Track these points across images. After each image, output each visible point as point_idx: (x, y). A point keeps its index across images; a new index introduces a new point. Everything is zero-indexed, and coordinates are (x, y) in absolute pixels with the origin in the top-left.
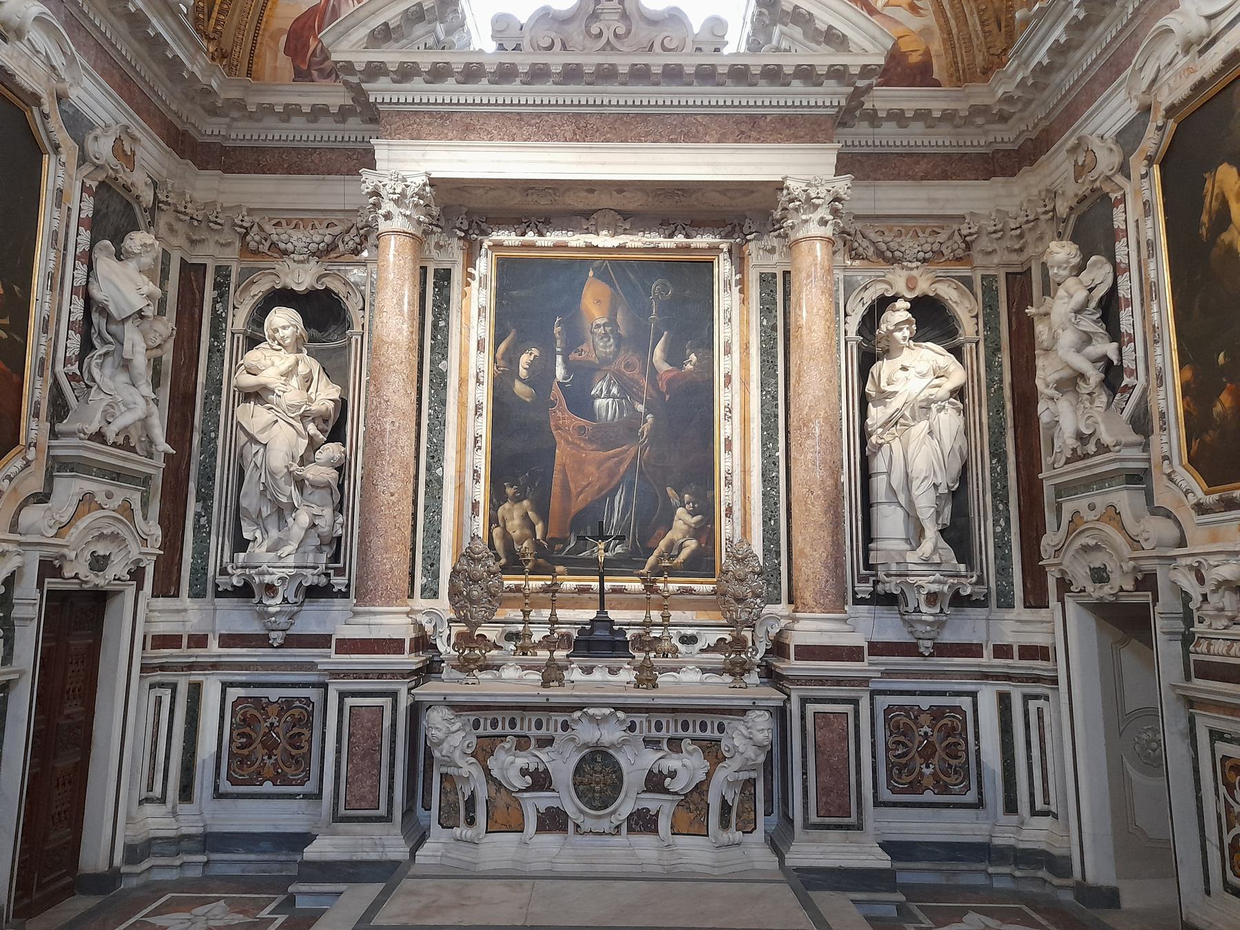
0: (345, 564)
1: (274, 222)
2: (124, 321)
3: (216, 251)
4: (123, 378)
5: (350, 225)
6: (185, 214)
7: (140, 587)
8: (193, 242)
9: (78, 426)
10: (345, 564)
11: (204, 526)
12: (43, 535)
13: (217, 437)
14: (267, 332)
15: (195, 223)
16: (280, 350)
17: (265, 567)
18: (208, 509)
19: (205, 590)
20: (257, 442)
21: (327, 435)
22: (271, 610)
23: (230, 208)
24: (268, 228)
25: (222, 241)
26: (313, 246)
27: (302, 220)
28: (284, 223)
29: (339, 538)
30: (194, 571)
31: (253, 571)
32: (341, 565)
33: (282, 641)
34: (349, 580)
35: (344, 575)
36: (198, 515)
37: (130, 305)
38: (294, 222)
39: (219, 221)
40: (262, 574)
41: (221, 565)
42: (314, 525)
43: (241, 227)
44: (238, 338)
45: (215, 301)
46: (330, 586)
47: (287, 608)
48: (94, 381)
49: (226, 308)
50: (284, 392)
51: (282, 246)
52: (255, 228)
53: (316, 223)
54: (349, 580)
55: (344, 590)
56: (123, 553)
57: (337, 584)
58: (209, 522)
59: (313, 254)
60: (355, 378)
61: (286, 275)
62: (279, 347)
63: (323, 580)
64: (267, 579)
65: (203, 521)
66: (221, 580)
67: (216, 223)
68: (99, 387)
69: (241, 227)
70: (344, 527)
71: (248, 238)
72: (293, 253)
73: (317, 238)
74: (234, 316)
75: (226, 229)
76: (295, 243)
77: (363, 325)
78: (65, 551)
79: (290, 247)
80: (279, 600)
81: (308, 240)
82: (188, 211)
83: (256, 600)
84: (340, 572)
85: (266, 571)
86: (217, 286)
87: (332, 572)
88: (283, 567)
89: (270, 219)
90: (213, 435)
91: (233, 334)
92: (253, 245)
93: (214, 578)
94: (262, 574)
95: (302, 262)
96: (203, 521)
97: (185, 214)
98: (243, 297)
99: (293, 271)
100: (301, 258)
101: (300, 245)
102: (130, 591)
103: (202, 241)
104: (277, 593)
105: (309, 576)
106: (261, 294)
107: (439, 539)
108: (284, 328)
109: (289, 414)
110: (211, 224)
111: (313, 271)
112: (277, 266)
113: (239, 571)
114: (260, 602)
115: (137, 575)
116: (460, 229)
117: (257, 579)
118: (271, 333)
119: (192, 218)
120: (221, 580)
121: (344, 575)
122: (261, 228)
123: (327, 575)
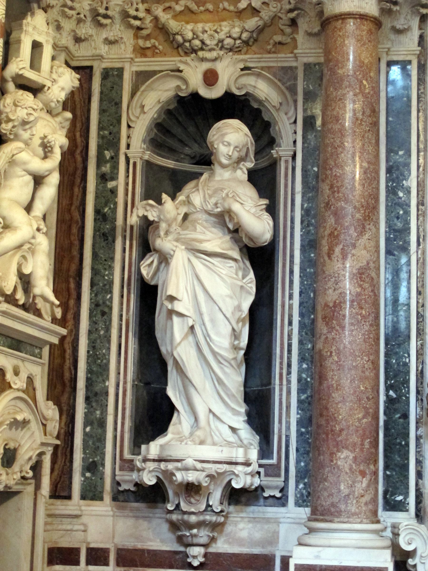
3: (104, 49)
7: (38, 487)
8: (78, 40)
17: (190, 462)
25: (111, 38)
26: (228, 41)
32: (274, 461)
33: (202, 560)
35: (279, 476)
39: (109, 13)
40: (186, 469)
55: (278, 495)
72: (202, 49)
79: (197, 43)
93: (114, 475)
94: (186, 469)
100: (214, 54)
102: (30, 489)
105: (242, 476)
121: (279, 476)
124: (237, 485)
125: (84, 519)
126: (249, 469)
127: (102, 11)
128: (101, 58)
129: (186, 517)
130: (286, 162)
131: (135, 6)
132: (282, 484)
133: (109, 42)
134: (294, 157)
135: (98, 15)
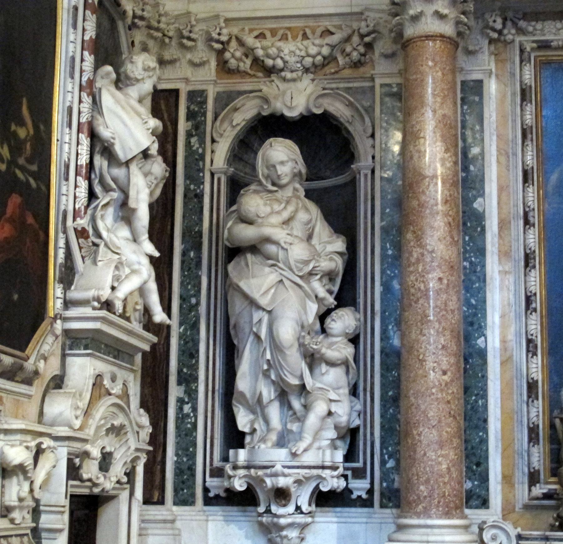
0: (365, 463)
1: (256, 33)
2: (127, 164)
3: (188, 72)
4: (124, 232)
5: (350, 32)
6: (158, 29)
7: (132, 494)
9: (90, 294)
10: (365, 463)
11: (188, 415)
12: (71, 427)
13: (198, 304)
14: (261, 170)
15: (167, 40)
16: (276, 191)
17: (278, 468)
18: (192, 394)
19: (193, 495)
20: (259, 307)
21: (334, 296)
22: (283, 521)
23: (204, 20)
24: (250, 40)
25: (197, 60)
26: (308, 61)
27: (289, 29)
28: (268, 34)
29: (357, 429)
30: (179, 471)
31: (260, 473)
32: (360, 465)
34: (372, 483)
36: (181, 402)
37: (138, 143)
38: (281, 32)
39: (193, 36)
40: (276, 475)
41: (211, 464)
42: (330, 414)
43: (218, 41)
44: (219, 180)
45: (189, 135)
46: (348, 491)
47: (300, 519)
48: (100, 236)
49: (202, 142)
50: (291, 244)
51: (269, 62)
52: (234, 44)
53: (308, 31)
54: (372, 483)
55: (364, 496)
56: (123, 449)
57: (358, 489)
58: (195, 409)
59: (307, 70)
60: (366, 223)
61: (276, 98)
62: (275, 188)
63: (342, 484)
64: (282, 482)
65: (187, 408)
66: (212, 482)
67: (189, 39)
68: (106, 245)
69: (218, 41)
70: (362, 416)
71: (227, 55)
73: (313, 50)
74: (213, 152)
75: (200, 45)
76: (287, 58)
77: (373, 157)
78: (88, 447)
80: (291, 508)
81: (303, 53)
82: (162, 26)
83: (261, 509)
84: (359, 474)
85: (280, 472)
86: (190, 116)
87: (349, 473)
88: (298, 467)
89: (251, 30)
90: (193, 301)
91: (212, 175)
92: (233, 63)
94: (276, 475)
95: (294, 80)
96: (187, 408)
97: (158, 29)
98: (223, 128)
99: (284, 93)
100: (294, 75)
101: (292, 60)
102: (125, 495)
103: (172, 62)
104: (289, 501)
105: (329, 479)
106: (244, 123)
107: (486, 431)
108: (282, 163)
109: (297, 273)
110: (185, 41)
111: (309, 91)
112: (265, 89)
113: (242, 472)
114: (268, 511)
115: (130, 475)
116: (494, 30)
117: (269, 482)
118: (266, 171)
119: (164, 35)
120: (212, 482)
122: (241, 43)
123: (345, 477)
124: (325, 488)
125: (178, 524)
126: (336, 473)
127: (186, 33)
128: (187, 80)
129: (275, 520)
130: (366, 175)
131: (218, 30)
132: (368, 486)
133: (194, 65)
134: (373, 172)
135: (183, 37)
